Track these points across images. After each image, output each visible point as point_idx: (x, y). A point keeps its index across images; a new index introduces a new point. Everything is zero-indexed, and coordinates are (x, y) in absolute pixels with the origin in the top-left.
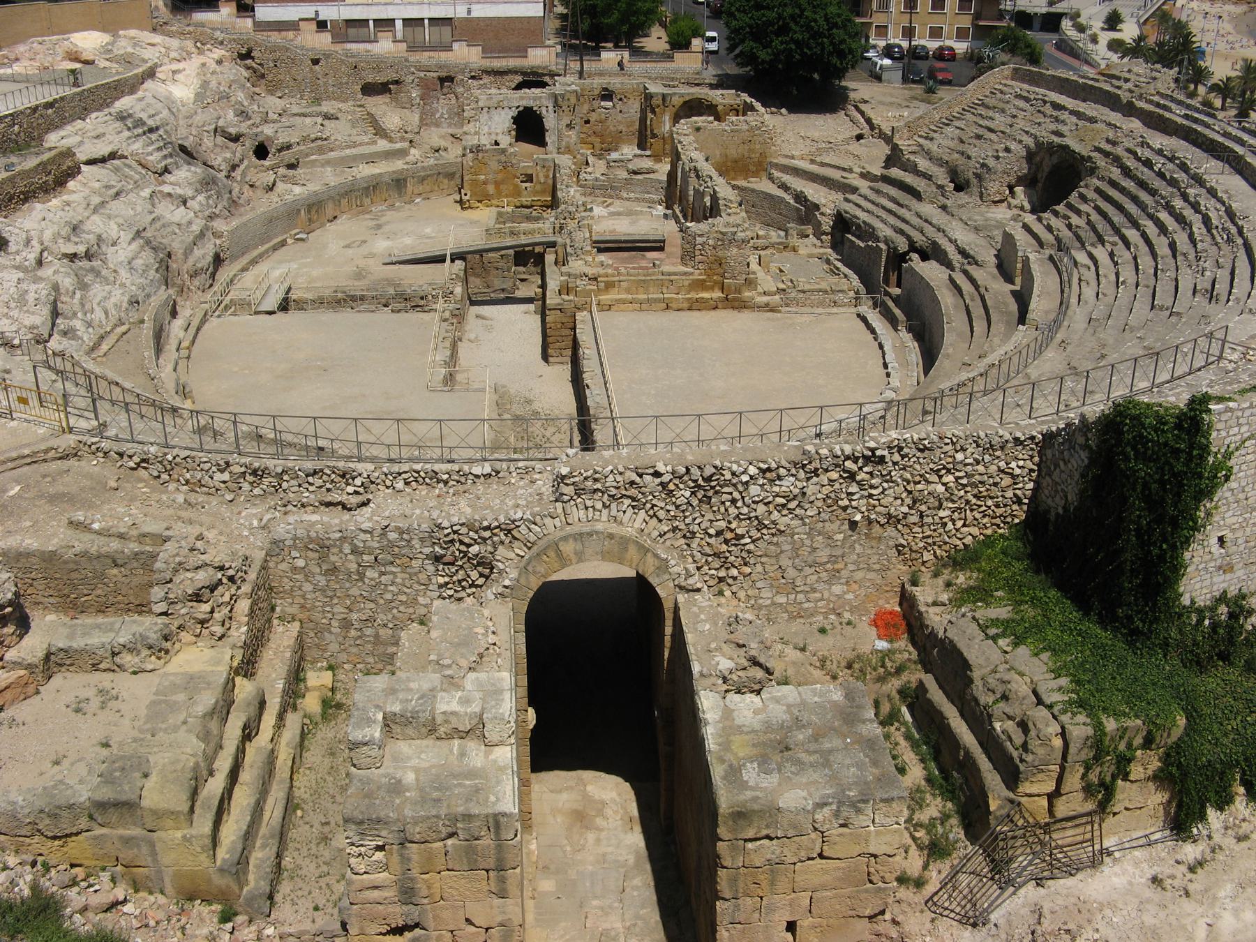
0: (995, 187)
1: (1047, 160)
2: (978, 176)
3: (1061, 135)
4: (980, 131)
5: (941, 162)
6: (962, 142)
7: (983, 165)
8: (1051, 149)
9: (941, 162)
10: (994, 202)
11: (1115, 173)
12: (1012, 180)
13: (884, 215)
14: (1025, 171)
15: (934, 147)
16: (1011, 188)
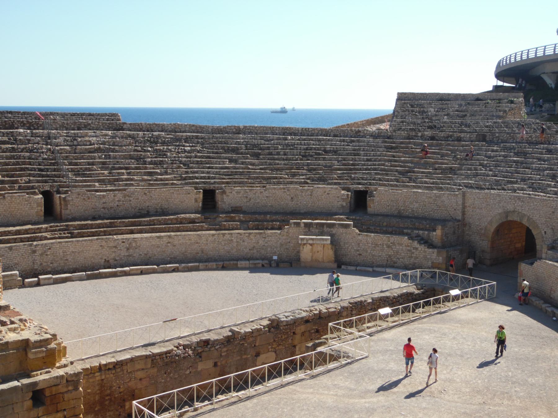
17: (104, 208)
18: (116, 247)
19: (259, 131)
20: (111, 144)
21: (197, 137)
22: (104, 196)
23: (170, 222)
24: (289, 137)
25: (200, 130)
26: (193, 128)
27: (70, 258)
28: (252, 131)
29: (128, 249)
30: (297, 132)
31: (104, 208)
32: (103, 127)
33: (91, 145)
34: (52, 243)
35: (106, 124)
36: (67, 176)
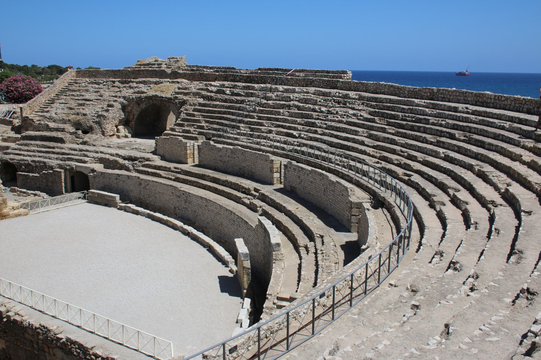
0: (110, 127)
1: (136, 107)
2: (99, 123)
3: (144, 93)
4: (80, 102)
5: (64, 121)
6: (71, 109)
7: (99, 116)
8: (139, 101)
9: (64, 121)
10: (110, 136)
11: (201, 101)
12: (117, 122)
13: (45, 155)
14: (123, 116)
15: (54, 115)
16: (116, 126)
17: (220, 161)
18: (179, 197)
19: (452, 97)
20: (304, 101)
21: (376, 100)
22: (220, 148)
23: (233, 186)
24: (461, 106)
25: (398, 92)
26: (392, 89)
27: (157, 196)
28: (445, 96)
29: (185, 202)
30: (489, 101)
31: (220, 161)
32: (323, 84)
33: (290, 101)
34: (149, 180)
35: (325, 81)
36: (238, 128)
